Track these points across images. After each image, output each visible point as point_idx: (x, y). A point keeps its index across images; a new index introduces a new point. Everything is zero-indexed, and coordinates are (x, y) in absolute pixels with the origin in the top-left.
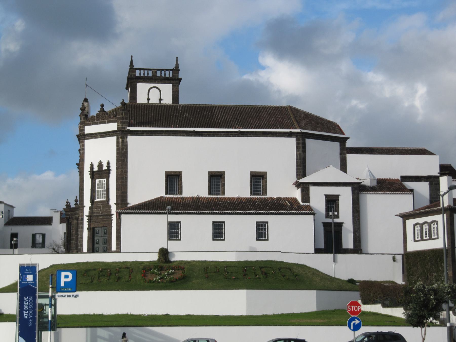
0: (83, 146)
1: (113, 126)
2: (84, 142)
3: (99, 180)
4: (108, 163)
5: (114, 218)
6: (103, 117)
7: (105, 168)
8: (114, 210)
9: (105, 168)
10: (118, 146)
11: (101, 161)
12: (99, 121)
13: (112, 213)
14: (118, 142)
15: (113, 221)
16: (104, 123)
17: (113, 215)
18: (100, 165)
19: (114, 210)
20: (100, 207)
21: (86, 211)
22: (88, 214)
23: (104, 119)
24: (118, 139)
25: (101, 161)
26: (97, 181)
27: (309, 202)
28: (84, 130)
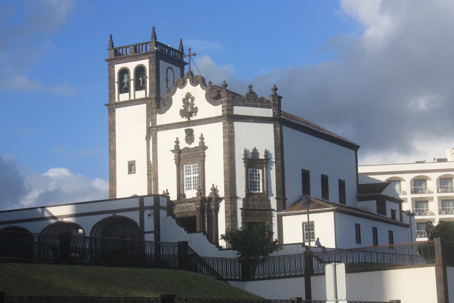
0: (232, 127)
1: (268, 113)
2: (233, 124)
3: (251, 169)
4: (267, 153)
5: (275, 214)
6: (255, 100)
7: (262, 156)
8: (274, 204)
9: (262, 156)
10: (275, 134)
11: (255, 148)
12: (250, 103)
13: (272, 208)
14: (275, 131)
15: (273, 218)
16: (257, 106)
17: (273, 210)
18: (255, 152)
19: (274, 204)
20: (256, 200)
21: (240, 204)
22: (242, 207)
23: (256, 103)
24: (275, 127)
25: (255, 148)
26: (249, 170)
27: (386, 215)
28: (232, 110)
